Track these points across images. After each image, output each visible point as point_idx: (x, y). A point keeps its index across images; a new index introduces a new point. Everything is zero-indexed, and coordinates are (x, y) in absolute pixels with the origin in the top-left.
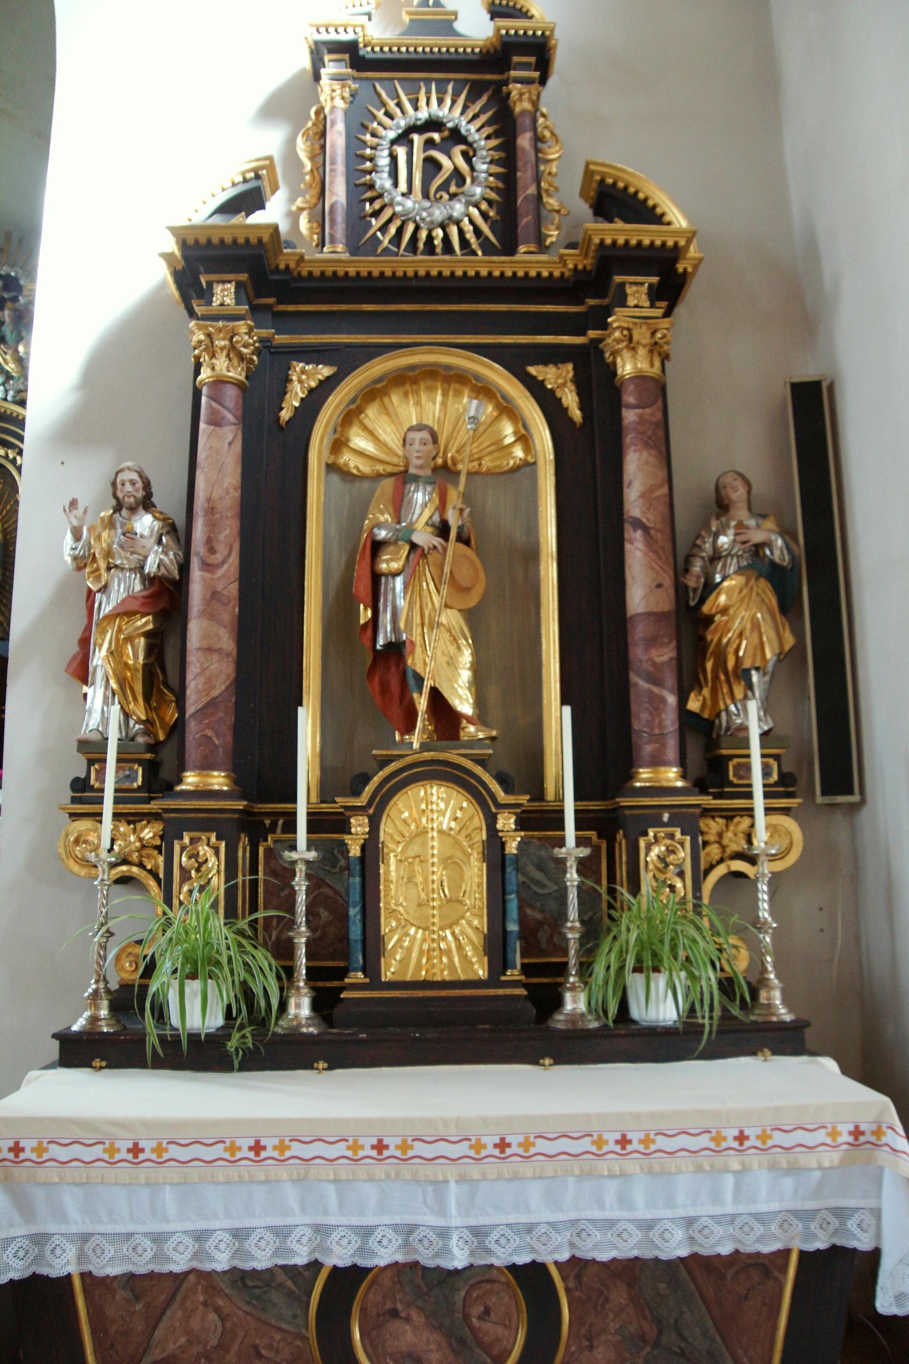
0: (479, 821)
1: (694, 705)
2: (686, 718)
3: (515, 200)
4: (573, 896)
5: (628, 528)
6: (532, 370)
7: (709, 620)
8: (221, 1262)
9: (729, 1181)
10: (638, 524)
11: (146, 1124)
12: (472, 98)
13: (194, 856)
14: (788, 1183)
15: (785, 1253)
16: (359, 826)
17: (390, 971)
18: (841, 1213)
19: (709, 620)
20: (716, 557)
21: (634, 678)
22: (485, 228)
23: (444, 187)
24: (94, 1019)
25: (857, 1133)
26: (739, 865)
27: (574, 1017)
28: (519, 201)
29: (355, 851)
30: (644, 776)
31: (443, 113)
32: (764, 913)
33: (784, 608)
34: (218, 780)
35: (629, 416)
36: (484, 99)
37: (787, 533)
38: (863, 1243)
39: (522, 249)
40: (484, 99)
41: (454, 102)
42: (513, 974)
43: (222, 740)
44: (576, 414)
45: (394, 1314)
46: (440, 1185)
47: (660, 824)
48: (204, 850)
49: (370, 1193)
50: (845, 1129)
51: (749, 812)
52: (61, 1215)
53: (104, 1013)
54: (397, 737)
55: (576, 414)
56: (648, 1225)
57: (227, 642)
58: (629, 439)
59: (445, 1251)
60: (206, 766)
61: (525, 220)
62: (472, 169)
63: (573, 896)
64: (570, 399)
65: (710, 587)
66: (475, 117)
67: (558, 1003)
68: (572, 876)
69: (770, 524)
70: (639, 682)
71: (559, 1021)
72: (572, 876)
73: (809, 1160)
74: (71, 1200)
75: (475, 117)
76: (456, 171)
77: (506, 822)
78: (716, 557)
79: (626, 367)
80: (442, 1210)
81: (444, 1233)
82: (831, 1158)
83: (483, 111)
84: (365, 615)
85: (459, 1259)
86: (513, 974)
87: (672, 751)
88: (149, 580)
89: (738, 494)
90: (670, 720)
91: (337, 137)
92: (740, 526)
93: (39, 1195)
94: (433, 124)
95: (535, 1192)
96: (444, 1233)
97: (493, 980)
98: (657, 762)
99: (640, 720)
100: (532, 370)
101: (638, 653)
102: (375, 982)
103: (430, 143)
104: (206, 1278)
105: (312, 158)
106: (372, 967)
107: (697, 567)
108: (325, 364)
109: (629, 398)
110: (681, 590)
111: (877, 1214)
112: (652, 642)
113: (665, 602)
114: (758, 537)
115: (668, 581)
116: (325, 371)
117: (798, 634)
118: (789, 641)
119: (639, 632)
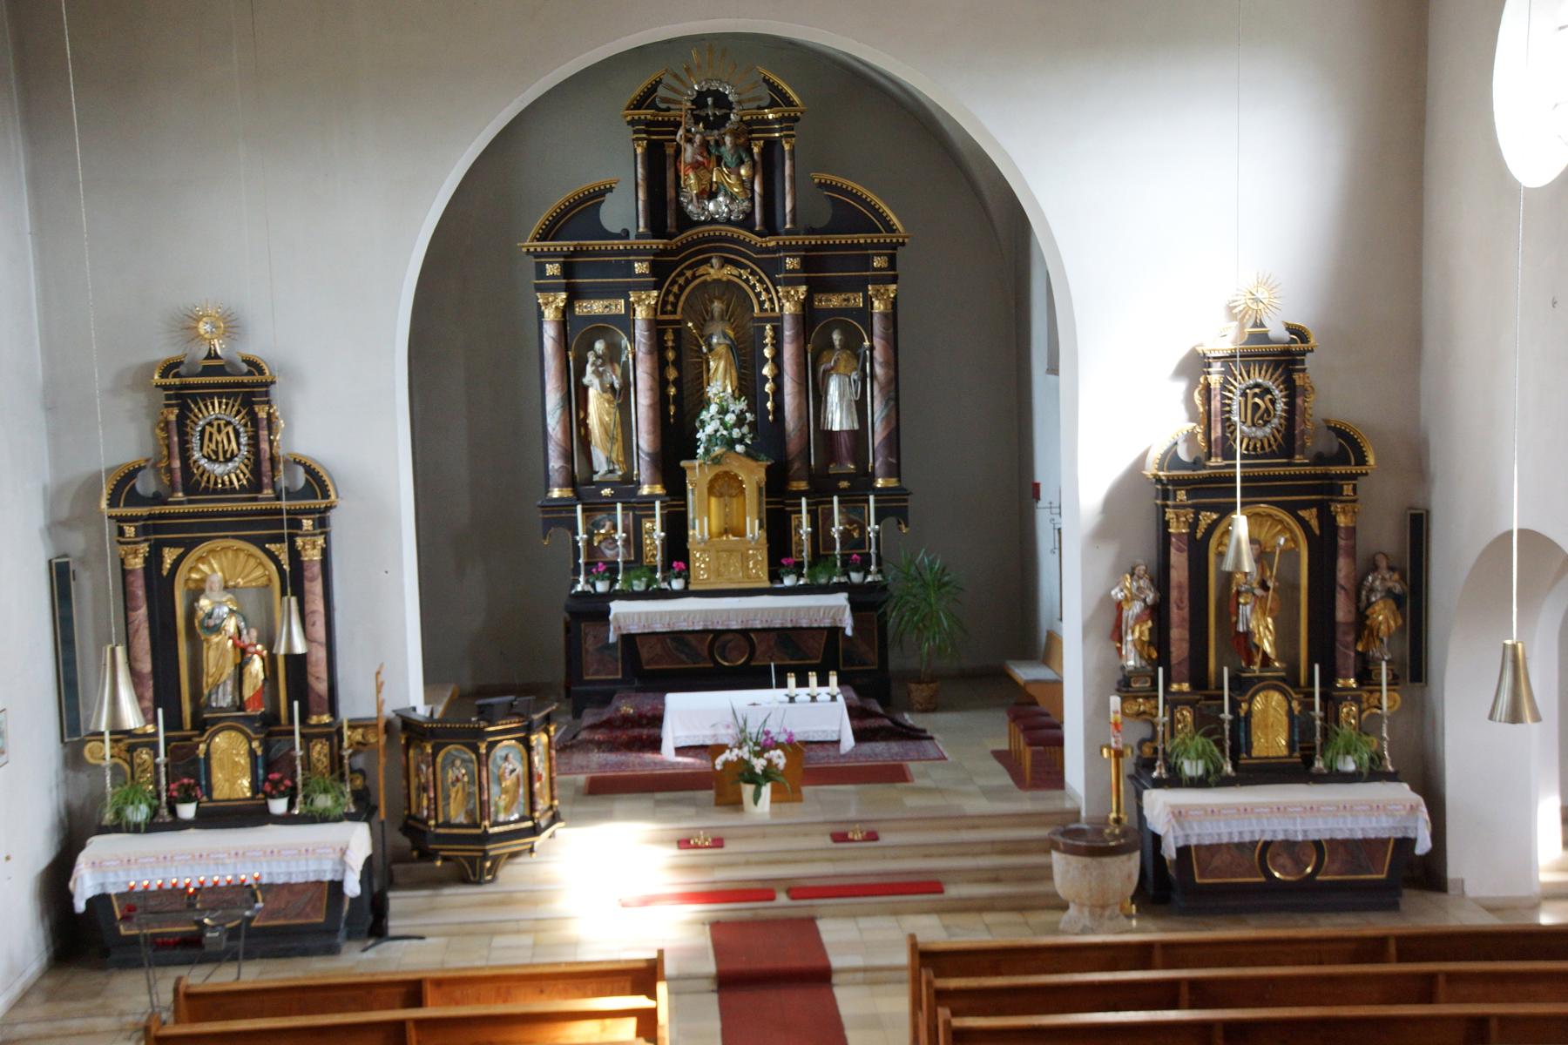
0: (1285, 704)
1: (1360, 648)
2: (1357, 652)
3: (1294, 430)
4: (1318, 729)
5: (1338, 589)
6: (1301, 513)
7: (1367, 617)
8: (1236, 839)
9: (1374, 819)
10: (1343, 588)
11: (1216, 805)
12: (1275, 370)
13: (1182, 714)
14: (1391, 820)
15: (1389, 839)
16: (1244, 706)
17: (1255, 753)
18: (1406, 828)
19: (1367, 617)
20: (1372, 590)
21: (1338, 645)
22: (1279, 437)
23: (1261, 418)
24: (1160, 773)
25: (1412, 806)
26: (1375, 710)
27: (1319, 769)
28: (1297, 432)
29: (1242, 714)
30: (1340, 683)
31: (1260, 381)
32: (1385, 735)
33: (1398, 608)
34: (1186, 687)
35: (1342, 543)
36: (1280, 370)
37: (1403, 577)
38: (1412, 835)
39: (1297, 457)
40: (1280, 370)
41: (1266, 372)
42: (1297, 754)
43: (1185, 671)
44: (1317, 532)
45: (1278, 854)
46: (1295, 819)
47: (1346, 699)
48: (1185, 712)
49: (1276, 821)
50: (1408, 807)
51: (1381, 691)
52: (1192, 829)
53: (1163, 771)
54: (1243, 664)
55: (1317, 532)
56: (1351, 830)
57: (1186, 634)
58: (1341, 552)
59: (1296, 836)
60: (1180, 682)
61: (1298, 443)
62: (1275, 409)
63: (1318, 729)
64: (1314, 523)
65: (1369, 604)
66: (1276, 380)
67: (1312, 763)
68: (1318, 722)
69: (1396, 576)
70: (1340, 648)
71: (1313, 770)
72: (1318, 722)
73: (1397, 813)
74: (1195, 825)
75: (1276, 380)
76: (1267, 410)
77: (1295, 704)
78: (1372, 590)
79: (1342, 521)
80: (1295, 824)
81: (1296, 832)
82: (1403, 813)
83: (1280, 376)
84: (1234, 619)
85: (1300, 838)
86: (1297, 754)
87: (1352, 672)
88: (1147, 606)
89: (1383, 563)
90: (1351, 662)
91: (1216, 404)
92: (1383, 579)
93: (1186, 825)
94: (1257, 385)
95: (1320, 821)
96: (1296, 832)
97: (1290, 756)
98: (1346, 677)
99: (1340, 661)
100: (1301, 513)
101: (1339, 636)
102: (1250, 757)
103: (1255, 395)
104: (1228, 845)
105: (1203, 405)
106: (1249, 752)
107: (1364, 593)
108: (1215, 513)
109: (1342, 534)
110: (1358, 608)
111: (1416, 828)
112: (1346, 633)
113: (1351, 618)
114: (1390, 584)
115: (1353, 609)
116: (1215, 516)
117: (1404, 621)
118: (1400, 622)
119: (1340, 630)
